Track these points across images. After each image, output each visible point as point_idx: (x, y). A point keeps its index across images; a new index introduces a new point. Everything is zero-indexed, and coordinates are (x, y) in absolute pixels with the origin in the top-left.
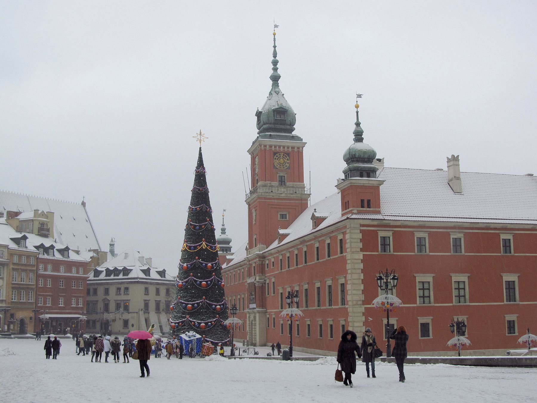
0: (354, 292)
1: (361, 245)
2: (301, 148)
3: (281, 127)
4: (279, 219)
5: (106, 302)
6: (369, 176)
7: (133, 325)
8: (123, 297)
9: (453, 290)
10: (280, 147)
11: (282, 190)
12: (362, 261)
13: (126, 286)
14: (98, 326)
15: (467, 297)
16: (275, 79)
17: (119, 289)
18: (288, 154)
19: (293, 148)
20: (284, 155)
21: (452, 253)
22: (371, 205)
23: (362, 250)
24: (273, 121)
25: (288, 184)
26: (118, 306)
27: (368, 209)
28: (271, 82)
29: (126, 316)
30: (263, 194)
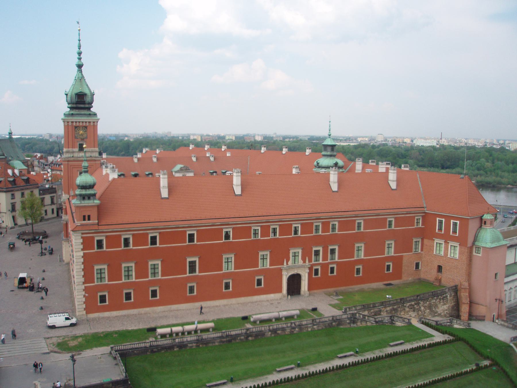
0: (78, 277)
1: (82, 247)
2: (96, 123)
3: (82, 106)
6: (89, 198)
9: (150, 270)
11: (82, 154)
12: (83, 257)
15: (160, 273)
16: (80, 66)
18: (86, 127)
19: (89, 122)
22: (91, 218)
23: (82, 250)
27: (88, 222)
28: (77, 68)
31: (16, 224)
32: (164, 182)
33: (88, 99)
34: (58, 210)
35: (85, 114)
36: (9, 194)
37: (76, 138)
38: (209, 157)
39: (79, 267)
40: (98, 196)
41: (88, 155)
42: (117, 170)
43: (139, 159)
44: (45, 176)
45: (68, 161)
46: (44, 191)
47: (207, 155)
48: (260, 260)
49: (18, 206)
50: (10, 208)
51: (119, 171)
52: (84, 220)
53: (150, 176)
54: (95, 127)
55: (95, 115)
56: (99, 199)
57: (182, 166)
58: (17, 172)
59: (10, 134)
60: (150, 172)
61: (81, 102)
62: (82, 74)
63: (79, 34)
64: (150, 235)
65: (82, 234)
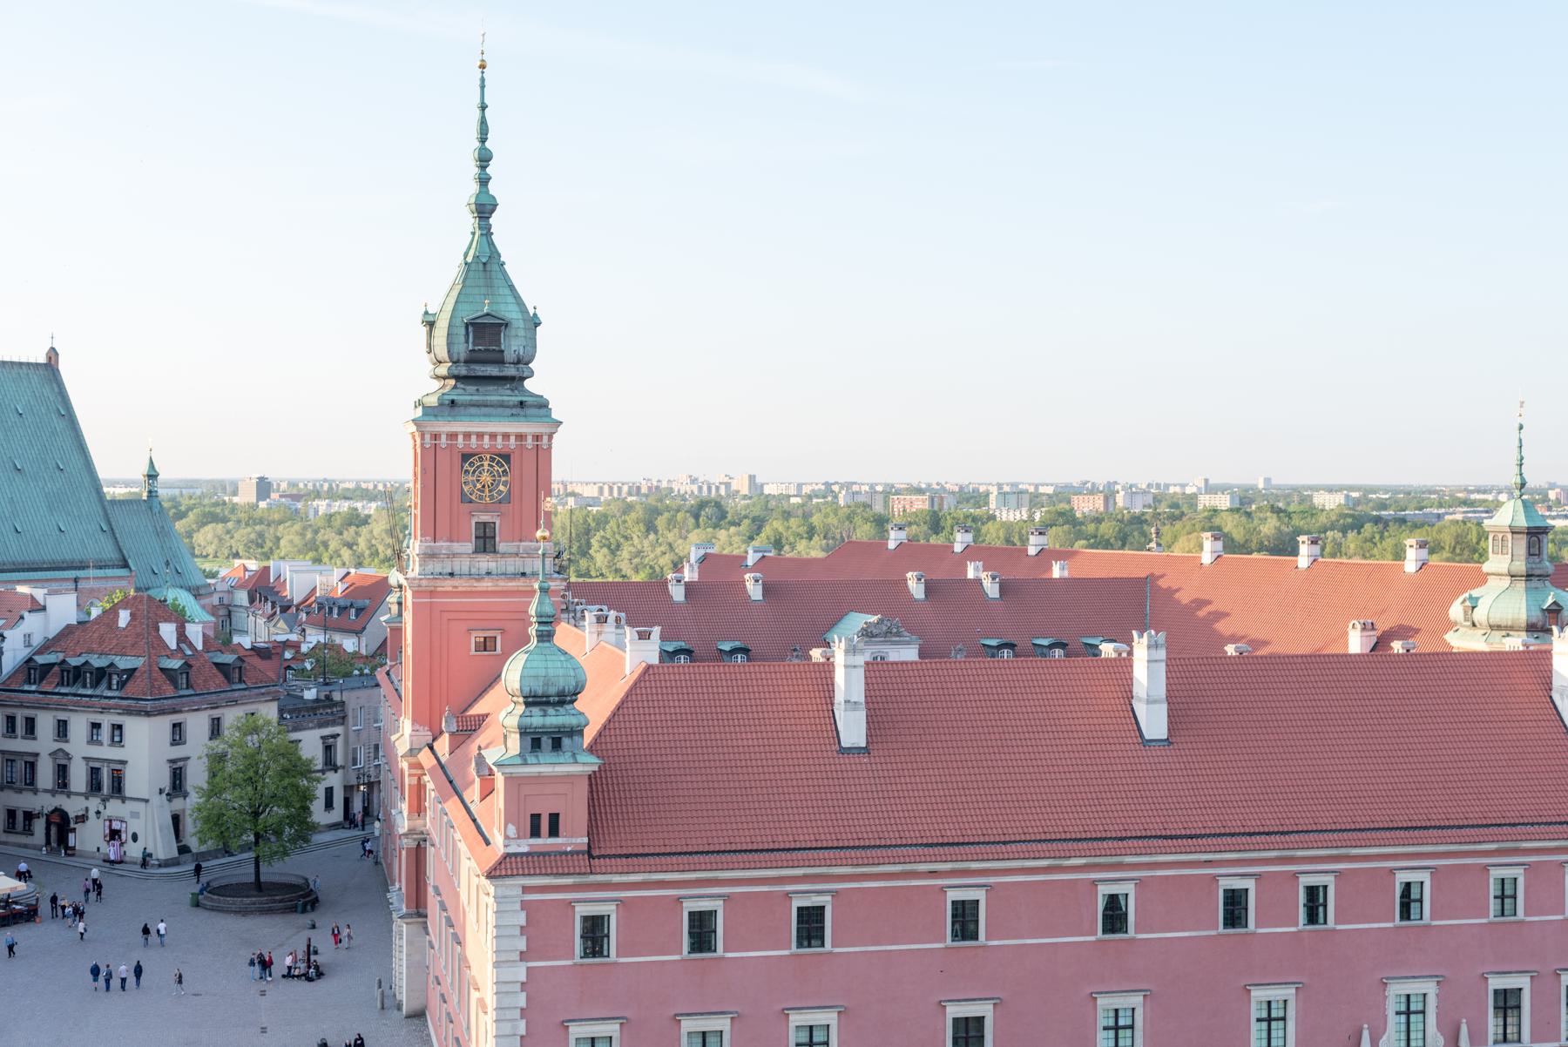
1: (522, 944)
2: (545, 438)
4: (473, 652)
5: (63, 762)
6: (557, 745)
7: (135, 838)
8: (107, 752)
10: (480, 436)
11: (485, 563)
13: (118, 719)
14: (39, 826)
16: (484, 210)
17: (96, 726)
18: (506, 457)
20: (492, 460)
21: (794, 949)
23: (523, 956)
24: (463, 356)
25: (502, 547)
26: (94, 773)
29: (114, 808)
30: (424, 583)
31: (184, 850)
32: (848, 682)
33: (512, 346)
34: (349, 789)
35: (502, 405)
36: (165, 722)
37: (465, 499)
38: (978, 581)
39: (507, 1028)
40: (589, 735)
41: (512, 565)
42: (656, 631)
43: (690, 588)
44: (288, 655)
45: (432, 594)
46: (297, 713)
47: (971, 574)
48: (1254, 1026)
49: (197, 776)
50: (166, 783)
51: (663, 638)
52: (535, 832)
53: (1058, 652)
54: (541, 453)
55: (543, 405)
56: (591, 749)
57: (874, 619)
58: (195, 633)
59: (152, 476)
60: (737, 644)
61: (487, 352)
62: (491, 244)
63: (483, 80)
64: (797, 903)
65: (526, 890)
